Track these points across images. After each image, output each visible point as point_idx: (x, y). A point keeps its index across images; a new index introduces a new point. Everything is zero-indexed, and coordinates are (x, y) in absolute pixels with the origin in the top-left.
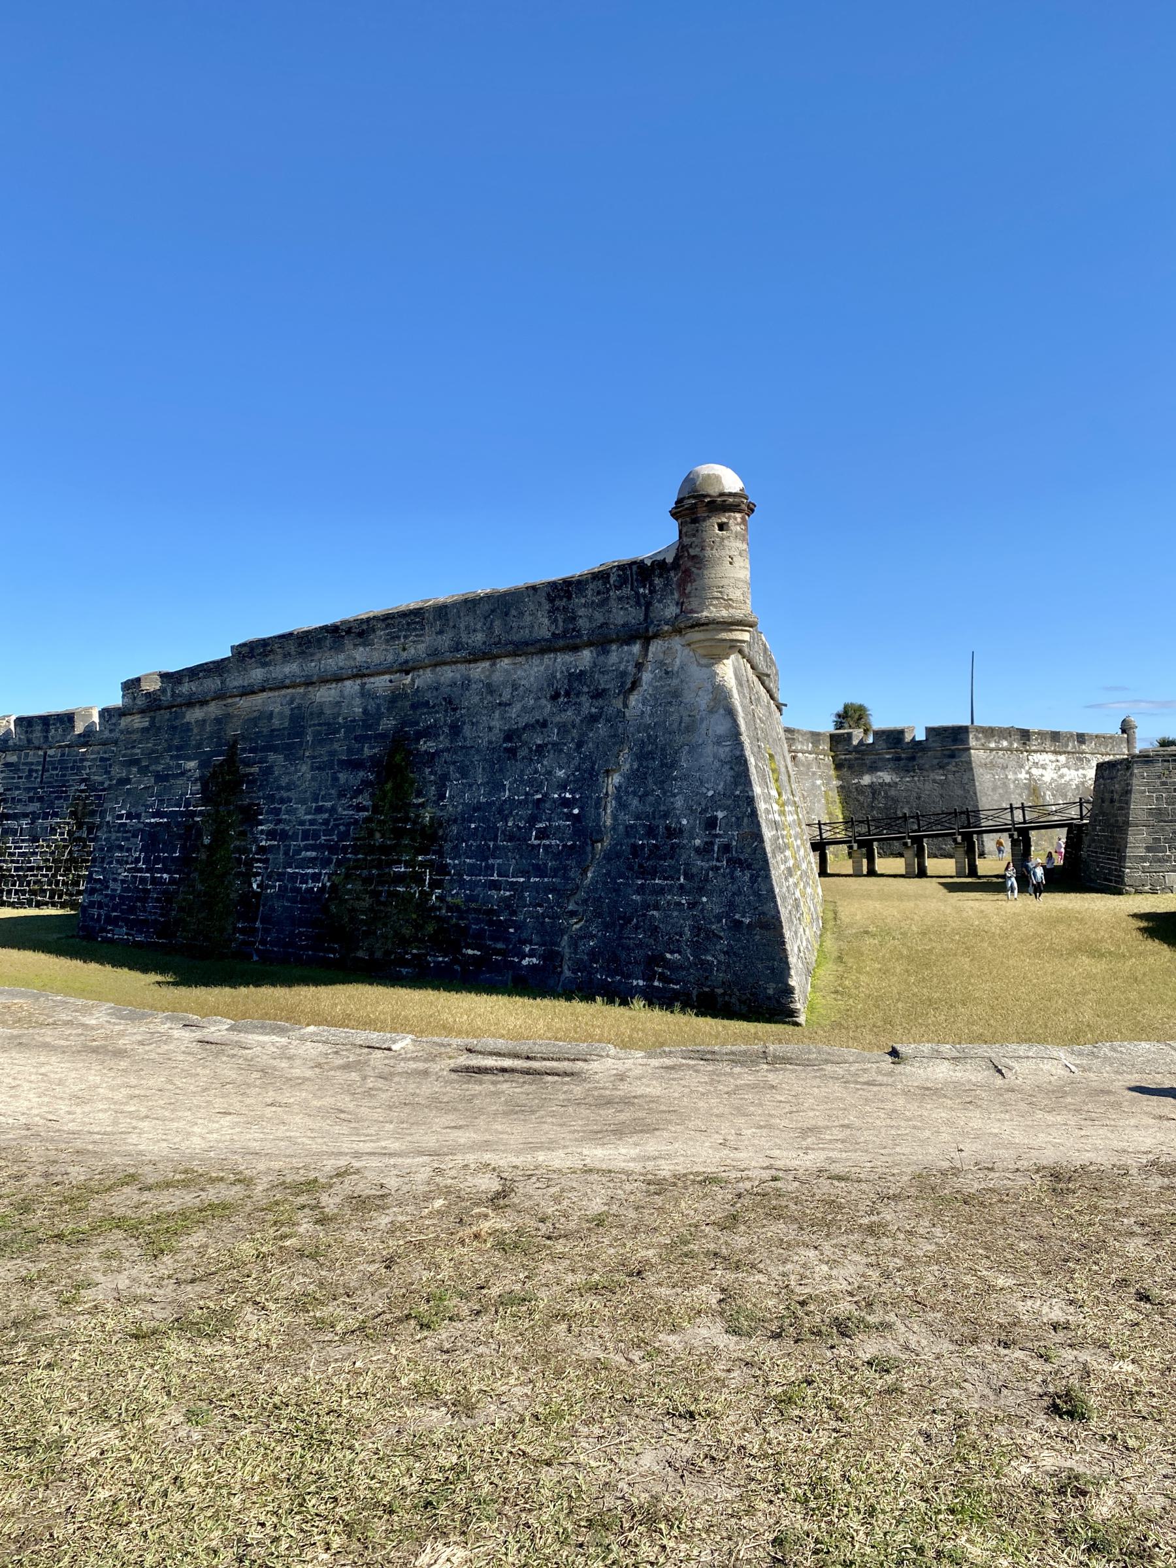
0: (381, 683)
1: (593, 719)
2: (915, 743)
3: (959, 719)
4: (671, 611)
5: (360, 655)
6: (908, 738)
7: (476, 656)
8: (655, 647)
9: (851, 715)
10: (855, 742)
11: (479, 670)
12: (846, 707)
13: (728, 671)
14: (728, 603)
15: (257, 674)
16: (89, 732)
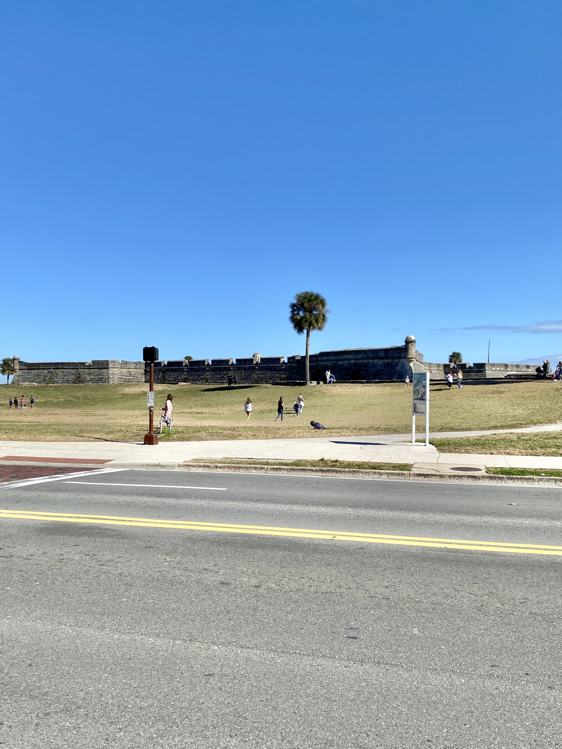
0: (353, 361)
1: (391, 370)
2: (470, 367)
3: (485, 361)
4: (404, 355)
5: (348, 357)
6: (467, 366)
7: (371, 359)
8: (401, 360)
9: (455, 357)
10: (451, 367)
11: (371, 361)
12: (454, 353)
13: (411, 364)
14: (412, 355)
15: (325, 358)
16: (257, 364)
